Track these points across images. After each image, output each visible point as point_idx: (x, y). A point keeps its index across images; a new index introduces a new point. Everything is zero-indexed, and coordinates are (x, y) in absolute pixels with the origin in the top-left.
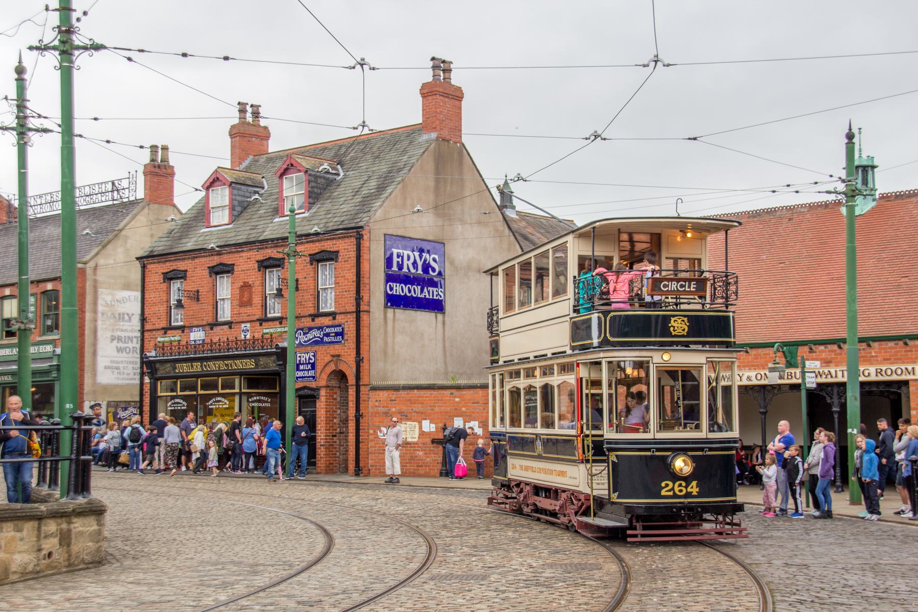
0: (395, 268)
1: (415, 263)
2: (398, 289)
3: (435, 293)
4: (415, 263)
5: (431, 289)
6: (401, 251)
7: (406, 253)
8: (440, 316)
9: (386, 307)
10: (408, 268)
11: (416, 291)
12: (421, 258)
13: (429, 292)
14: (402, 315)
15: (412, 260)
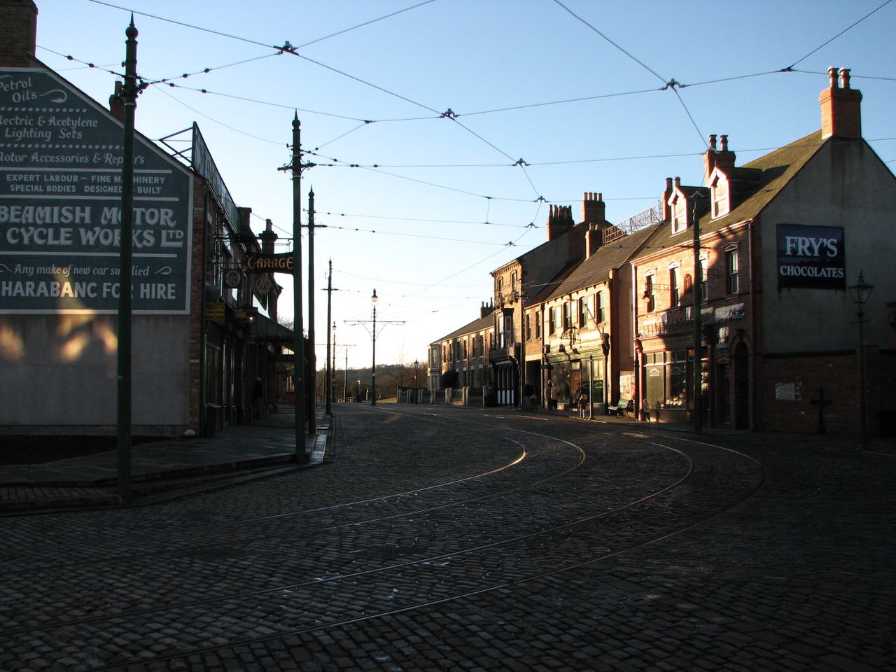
0: (789, 252)
1: (811, 249)
2: (792, 271)
3: (834, 272)
4: (811, 249)
5: (829, 269)
6: (795, 238)
7: (800, 239)
8: (840, 293)
9: (780, 288)
10: (803, 252)
11: (814, 272)
12: (817, 244)
13: (827, 272)
14: (795, 292)
15: (807, 245)
